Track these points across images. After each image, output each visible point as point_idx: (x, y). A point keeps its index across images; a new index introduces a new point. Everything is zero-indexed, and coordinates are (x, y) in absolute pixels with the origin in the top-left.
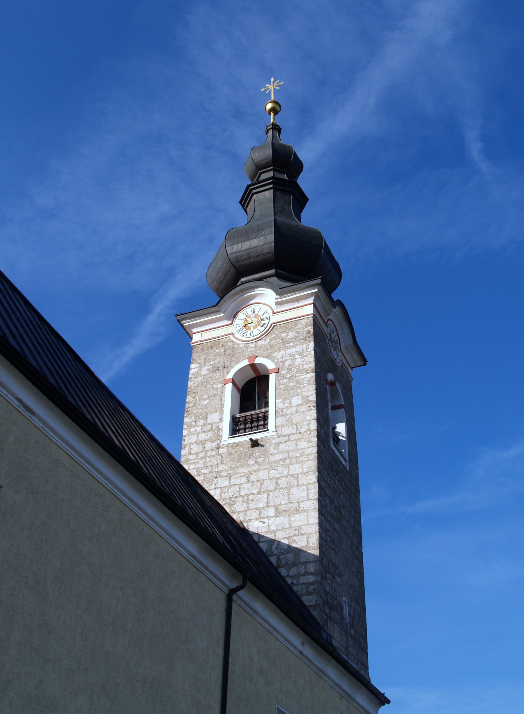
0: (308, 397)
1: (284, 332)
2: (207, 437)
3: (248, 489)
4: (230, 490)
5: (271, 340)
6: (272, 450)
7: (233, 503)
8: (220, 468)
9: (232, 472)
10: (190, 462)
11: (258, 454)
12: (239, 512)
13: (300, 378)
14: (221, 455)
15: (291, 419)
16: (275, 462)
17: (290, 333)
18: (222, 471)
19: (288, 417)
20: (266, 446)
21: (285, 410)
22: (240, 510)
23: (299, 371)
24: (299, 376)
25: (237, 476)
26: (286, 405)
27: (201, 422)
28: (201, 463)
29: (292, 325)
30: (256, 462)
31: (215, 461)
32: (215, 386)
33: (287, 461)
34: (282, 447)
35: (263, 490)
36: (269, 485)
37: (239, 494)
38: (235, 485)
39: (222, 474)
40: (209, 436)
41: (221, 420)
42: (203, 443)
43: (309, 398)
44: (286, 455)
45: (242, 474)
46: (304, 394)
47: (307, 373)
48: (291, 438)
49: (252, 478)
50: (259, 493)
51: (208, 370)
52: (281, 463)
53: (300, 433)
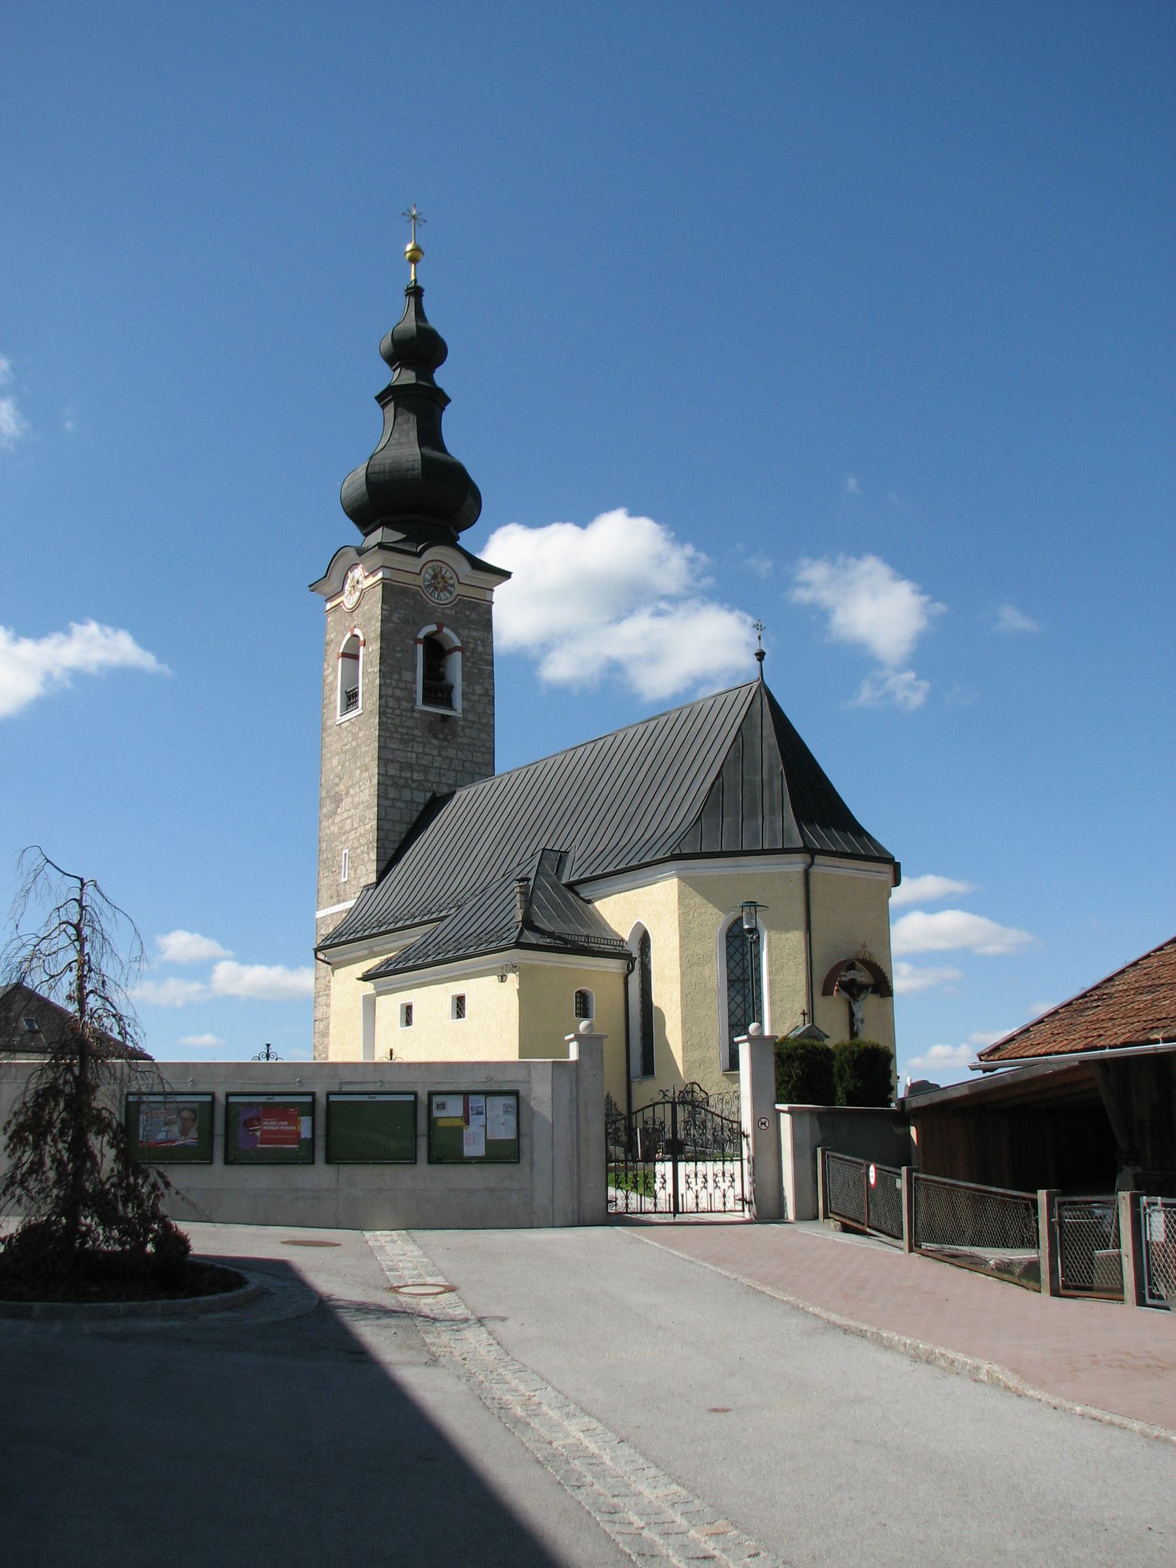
0: (488, 690)
3: (440, 762)
4: (425, 758)
8: (416, 732)
10: (389, 715)
14: (415, 718)
16: (462, 744)
17: (473, 614)
19: (472, 703)
21: (469, 695)
25: (430, 746)
28: (397, 721)
30: (446, 739)
31: (410, 723)
32: (407, 641)
33: (472, 747)
34: (467, 731)
37: (432, 764)
38: (429, 754)
39: (418, 739)
41: (414, 682)
42: (398, 699)
43: (490, 692)
48: (475, 726)
50: (449, 769)
51: (399, 618)
52: (466, 747)
53: (482, 723)
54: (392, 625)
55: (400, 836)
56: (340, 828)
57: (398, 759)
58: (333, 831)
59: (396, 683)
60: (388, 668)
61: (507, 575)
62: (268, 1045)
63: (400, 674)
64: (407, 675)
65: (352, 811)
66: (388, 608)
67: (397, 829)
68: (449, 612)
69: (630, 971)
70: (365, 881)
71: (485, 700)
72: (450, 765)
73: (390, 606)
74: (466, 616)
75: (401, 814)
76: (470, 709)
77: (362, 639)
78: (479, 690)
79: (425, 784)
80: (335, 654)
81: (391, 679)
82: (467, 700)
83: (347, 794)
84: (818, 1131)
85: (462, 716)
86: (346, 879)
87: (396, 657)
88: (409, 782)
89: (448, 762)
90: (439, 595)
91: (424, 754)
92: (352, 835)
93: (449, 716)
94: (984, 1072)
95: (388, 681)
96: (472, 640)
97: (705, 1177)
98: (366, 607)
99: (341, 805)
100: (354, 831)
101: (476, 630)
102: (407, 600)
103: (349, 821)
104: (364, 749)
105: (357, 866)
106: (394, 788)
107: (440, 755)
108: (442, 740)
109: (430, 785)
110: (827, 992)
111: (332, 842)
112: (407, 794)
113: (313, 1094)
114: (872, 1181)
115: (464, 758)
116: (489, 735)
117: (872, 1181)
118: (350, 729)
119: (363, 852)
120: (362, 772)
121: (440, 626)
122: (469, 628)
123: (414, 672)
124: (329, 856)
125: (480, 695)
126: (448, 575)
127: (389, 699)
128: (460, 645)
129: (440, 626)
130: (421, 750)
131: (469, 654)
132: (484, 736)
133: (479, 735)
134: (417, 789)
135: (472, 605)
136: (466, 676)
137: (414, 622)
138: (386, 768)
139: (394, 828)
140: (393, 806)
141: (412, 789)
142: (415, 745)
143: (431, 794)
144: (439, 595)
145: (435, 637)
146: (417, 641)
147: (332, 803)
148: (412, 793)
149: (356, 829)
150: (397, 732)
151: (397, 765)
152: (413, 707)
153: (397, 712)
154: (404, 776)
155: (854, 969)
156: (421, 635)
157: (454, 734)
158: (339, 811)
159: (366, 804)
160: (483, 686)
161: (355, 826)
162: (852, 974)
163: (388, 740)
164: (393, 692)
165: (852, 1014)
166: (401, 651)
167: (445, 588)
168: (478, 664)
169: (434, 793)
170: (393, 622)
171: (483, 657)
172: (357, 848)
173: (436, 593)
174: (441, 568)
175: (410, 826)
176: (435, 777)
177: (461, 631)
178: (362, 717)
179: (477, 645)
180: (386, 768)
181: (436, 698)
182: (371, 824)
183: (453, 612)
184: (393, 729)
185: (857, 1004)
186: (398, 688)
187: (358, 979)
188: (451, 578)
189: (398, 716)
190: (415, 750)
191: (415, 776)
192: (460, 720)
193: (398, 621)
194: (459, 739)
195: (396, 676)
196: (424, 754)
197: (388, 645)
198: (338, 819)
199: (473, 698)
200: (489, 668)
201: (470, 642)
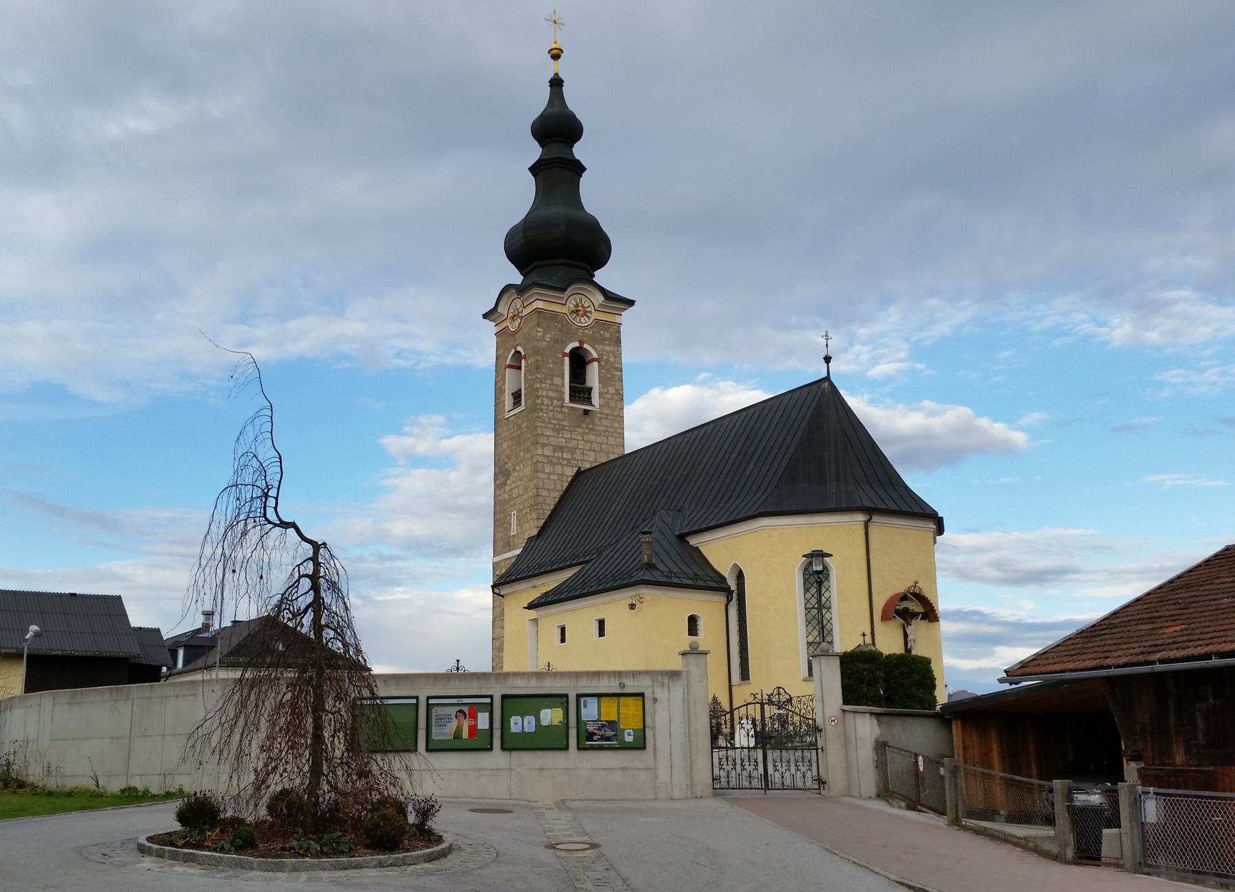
0: (619, 390)
6: (597, 421)
8: (565, 423)
9: (572, 428)
11: (588, 421)
12: (578, 460)
15: (608, 403)
16: (600, 431)
18: (566, 426)
21: (605, 394)
23: (613, 367)
27: (549, 381)
28: (551, 414)
31: (560, 416)
32: (557, 355)
34: (603, 421)
36: (595, 446)
38: (575, 439)
41: (563, 385)
42: (551, 399)
44: (605, 428)
46: (616, 387)
47: (618, 371)
48: (609, 417)
50: (590, 450)
51: (550, 338)
52: (603, 433)
54: (545, 343)
56: (509, 496)
61: (631, 303)
62: (458, 661)
63: (552, 380)
64: (557, 381)
67: (552, 495)
69: (729, 601)
71: (616, 397)
73: (544, 329)
74: (601, 335)
75: (555, 484)
77: (523, 354)
78: (611, 390)
80: (503, 366)
81: (546, 383)
82: (603, 398)
83: (514, 469)
84: (877, 728)
86: (515, 533)
87: (550, 368)
88: (561, 460)
90: (580, 319)
91: (571, 439)
92: (518, 501)
93: (589, 411)
94: (1011, 685)
95: (543, 385)
96: (605, 353)
97: (734, 760)
98: (525, 330)
100: (520, 498)
101: (609, 345)
103: (516, 490)
107: (583, 440)
109: (576, 462)
110: (885, 618)
112: (559, 469)
113: (491, 697)
114: (921, 769)
115: (602, 442)
116: (620, 424)
117: (921, 769)
119: (526, 513)
120: (525, 453)
121: (581, 342)
122: (603, 344)
123: (563, 378)
125: (612, 394)
126: (586, 305)
127: (544, 399)
129: (581, 342)
130: (569, 436)
131: (603, 363)
132: (616, 425)
133: (612, 424)
134: (566, 465)
135: (605, 326)
137: (562, 341)
140: (549, 478)
141: (562, 465)
142: (565, 432)
144: (580, 319)
145: (578, 352)
147: (503, 477)
148: (563, 469)
149: (521, 496)
150: (551, 423)
151: (551, 448)
154: (556, 456)
155: (907, 600)
156: (567, 350)
158: (508, 482)
161: (521, 493)
162: (905, 604)
163: (544, 430)
164: (547, 393)
165: (906, 636)
166: (553, 363)
167: (585, 314)
169: (579, 468)
172: (522, 510)
177: (597, 346)
178: (524, 413)
179: (609, 356)
181: (579, 398)
183: (591, 333)
185: (910, 627)
186: (551, 390)
187: (524, 608)
188: (589, 306)
189: (551, 411)
190: (564, 436)
191: (565, 455)
193: (549, 340)
194: (598, 428)
195: (549, 381)
196: (571, 439)
198: (507, 488)
199: (607, 396)
200: (619, 373)
201: (605, 355)
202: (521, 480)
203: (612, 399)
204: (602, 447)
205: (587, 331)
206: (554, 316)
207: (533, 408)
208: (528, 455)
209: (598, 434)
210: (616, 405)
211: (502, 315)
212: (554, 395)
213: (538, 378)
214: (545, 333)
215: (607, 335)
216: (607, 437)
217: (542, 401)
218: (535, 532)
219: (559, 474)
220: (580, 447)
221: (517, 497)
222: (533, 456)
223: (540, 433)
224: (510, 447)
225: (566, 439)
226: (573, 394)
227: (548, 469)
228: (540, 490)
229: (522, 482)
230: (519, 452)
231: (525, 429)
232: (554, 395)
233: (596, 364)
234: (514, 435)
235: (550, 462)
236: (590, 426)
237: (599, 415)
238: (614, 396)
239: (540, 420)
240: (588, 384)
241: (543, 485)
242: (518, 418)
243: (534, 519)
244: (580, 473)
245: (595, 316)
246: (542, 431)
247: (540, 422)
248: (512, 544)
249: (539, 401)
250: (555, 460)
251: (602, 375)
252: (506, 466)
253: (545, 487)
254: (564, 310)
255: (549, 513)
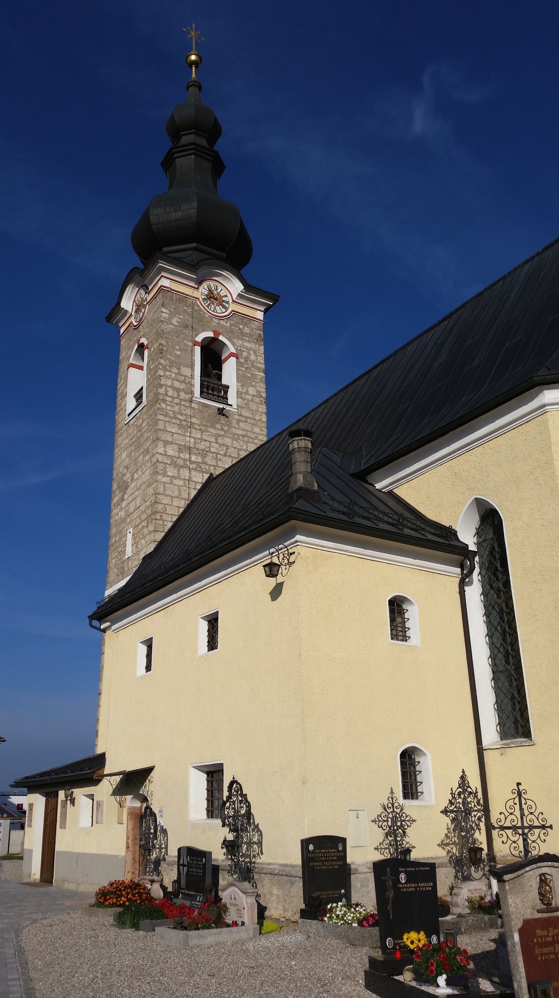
0: (260, 392)
1: (241, 324)
2: (180, 386)
4: (202, 443)
5: (231, 325)
7: (205, 456)
8: (194, 420)
12: (210, 465)
13: (254, 372)
14: (194, 408)
16: (237, 434)
17: (246, 328)
19: (246, 401)
20: (230, 418)
21: (243, 395)
22: (211, 464)
24: (254, 371)
25: (208, 434)
26: (245, 391)
28: (176, 409)
29: (247, 321)
30: (222, 429)
31: (188, 412)
32: (186, 342)
35: (228, 454)
37: (210, 450)
38: (207, 441)
39: (196, 426)
40: (183, 387)
41: (192, 377)
42: (178, 390)
43: (261, 394)
44: (244, 433)
45: (212, 434)
46: (258, 388)
47: (259, 372)
48: (249, 421)
49: (220, 441)
50: (225, 455)
52: (241, 438)
53: (255, 419)
54: (171, 326)
55: (178, 510)
57: (177, 442)
58: (121, 515)
59: (176, 376)
60: (168, 362)
63: (179, 369)
64: (186, 371)
65: (136, 493)
66: (168, 312)
68: (225, 324)
70: (145, 553)
72: (226, 452)
73: (170, 311)
74: (240, 329)
75: (179, 490)
76: (243, 406)
79: (203, 466)
81: (170, 371)
82: (242, 398)
85: (236, 411)
87: (176, 354)
88: (188, 463)
89: (225, 448)
90: (215, 308)
91: (202, 439)
92: (135, 515)
95: (167, 373)
96: (245, 350)
99: (127, 491)
100: (137, 511)
102: (186, 308)
103: (133, 503)
104: (146, 435)
105: (138, 541)
106: (172, 467)
107: (217, 442)
108: (219, 430)
109: (207, 468)
111: (120, 526)
112: (185, 473)
115: (240, 447)
118: (135, 424)
119: (143, 527)
120: (144, 457)
122: (242, 339)
124: (117, 539)
125: (253, 396)
127: (168, 389)
128: (235, 352)
129: (217, 333)
130: (199, 436)
131: (242, 361)
133: (252, 429)
134: (195, 470)
135: (245, 320)
136: (240, 378)
138: (165, 448)
139: (172, 503)
140: (171, 483)
142: (193, 431)
143: (209, 475)
144: (215, 308)
146: (196, 343)
149: (139, 508)
151: (176, 447)
152: (192, 398)
153: (177, 401)
154: (183, 457)
156: (199, 339)
157: (230, 425)
158: (126, 497)
159: (147, 483)
160: (256, 388)
161: (138, 504)
163: (167, 425)
164: (173, 383)
166: (180, 350)
168: (251, 369)
169: (211, 474)
170: (173, 325)
171: (255, 364)
172: (138, 525)
173: (213, 306)
174: (217, 286)
175: (187, 502)
176: (212, 460)
177: (235, 340)
178: (145, 410)
180: (165, 448)
181: (213, 395)
182: (150, 499)
183: (228, 325)
184: (172, 415)
186: (178, 380)
188: (226, 296)
189: (177, 404)
190: (192, 435)
191: (193, 458)
192: (235, 415)
193: (176, 324)
194: (234, 431)
195: (175, 370)
196: (202, 439)
197: (168, 343)
198: (124, 504)
199: (247, 397)
201: (244, 351)
202: (138, 489)
203: (252, 401)
204: (240, 452)
205: (222, 322)
206: (183, 298)
207: (155, 399)
208: (147, 457)
209: (236, 437)
210: (258, 408)
211: (126, 311)
212: (182, 386)
213: (161, 364)
214: (171, 315)
215: (247, 330)
216: (247, 442)
217: (166, 391)
218: (151, 548)
219: (185, 479)
220: (212, 450)
221: (134, 511)
222: (153, 455)
223: (162, 427)
224: (129, 456)
225: (195, 438)
226: (205, 390)
227: (171, 471)
228: (159, 497)
229: (140, 491)
230: (139, 456)
231: (145, 428)
232: (182, 386)
233: (233, 360)
234: (133, 440)
235: (174, 464)
236: (226, 428)
237: (237, 417)
238: (255, 398)
239: (161, 413)
240: (224, 381)
241: (165, 490)
242: (138, 418)
243: (151, 532)
244: (211, 479)
245: (232, 307)
246: (165, 426)
247: (163, 415)
248: (126, 569)
249: (162, 391)
250: (180, 462)
251: (240, 372)
252: (125, 478)
253: (168, 492)
254: (196, 294)
255: (170, 525)
